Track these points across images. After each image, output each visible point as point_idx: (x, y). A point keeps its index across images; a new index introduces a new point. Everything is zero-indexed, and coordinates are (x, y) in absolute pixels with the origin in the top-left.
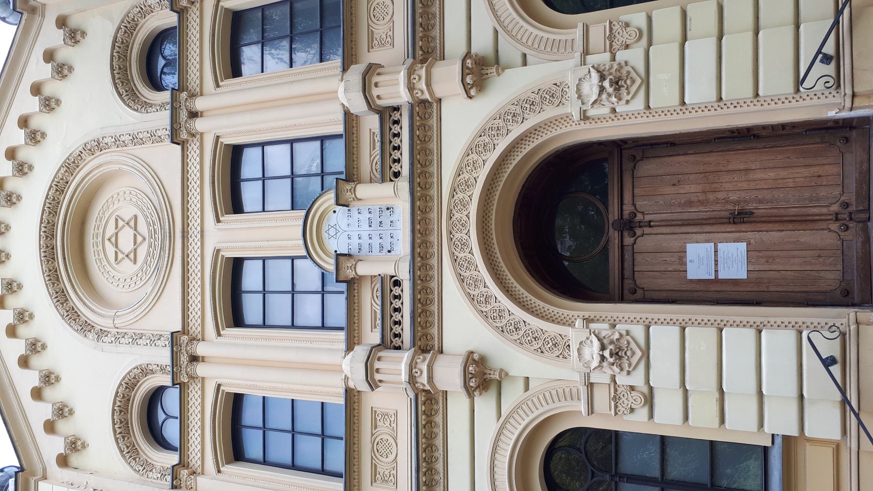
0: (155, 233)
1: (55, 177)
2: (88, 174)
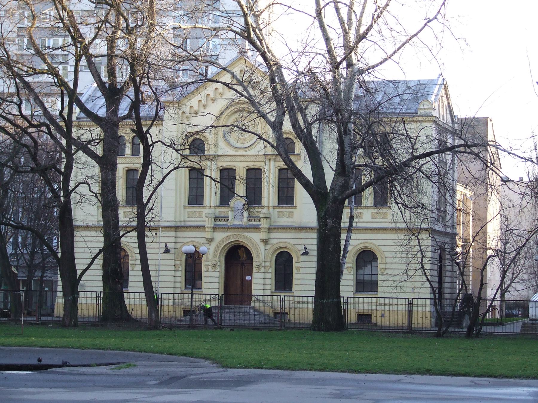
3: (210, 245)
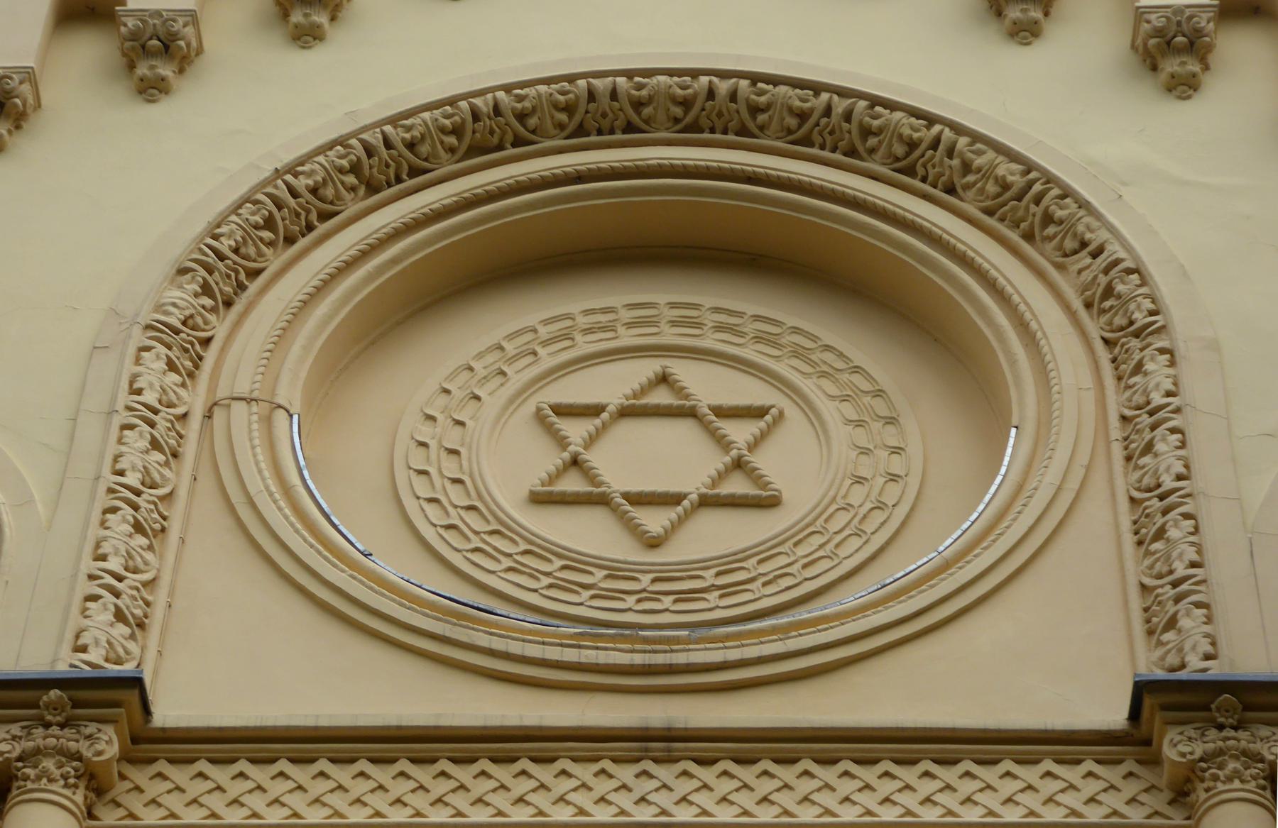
0: (682, 596)
1: (976, 137)
2: (991, 285)
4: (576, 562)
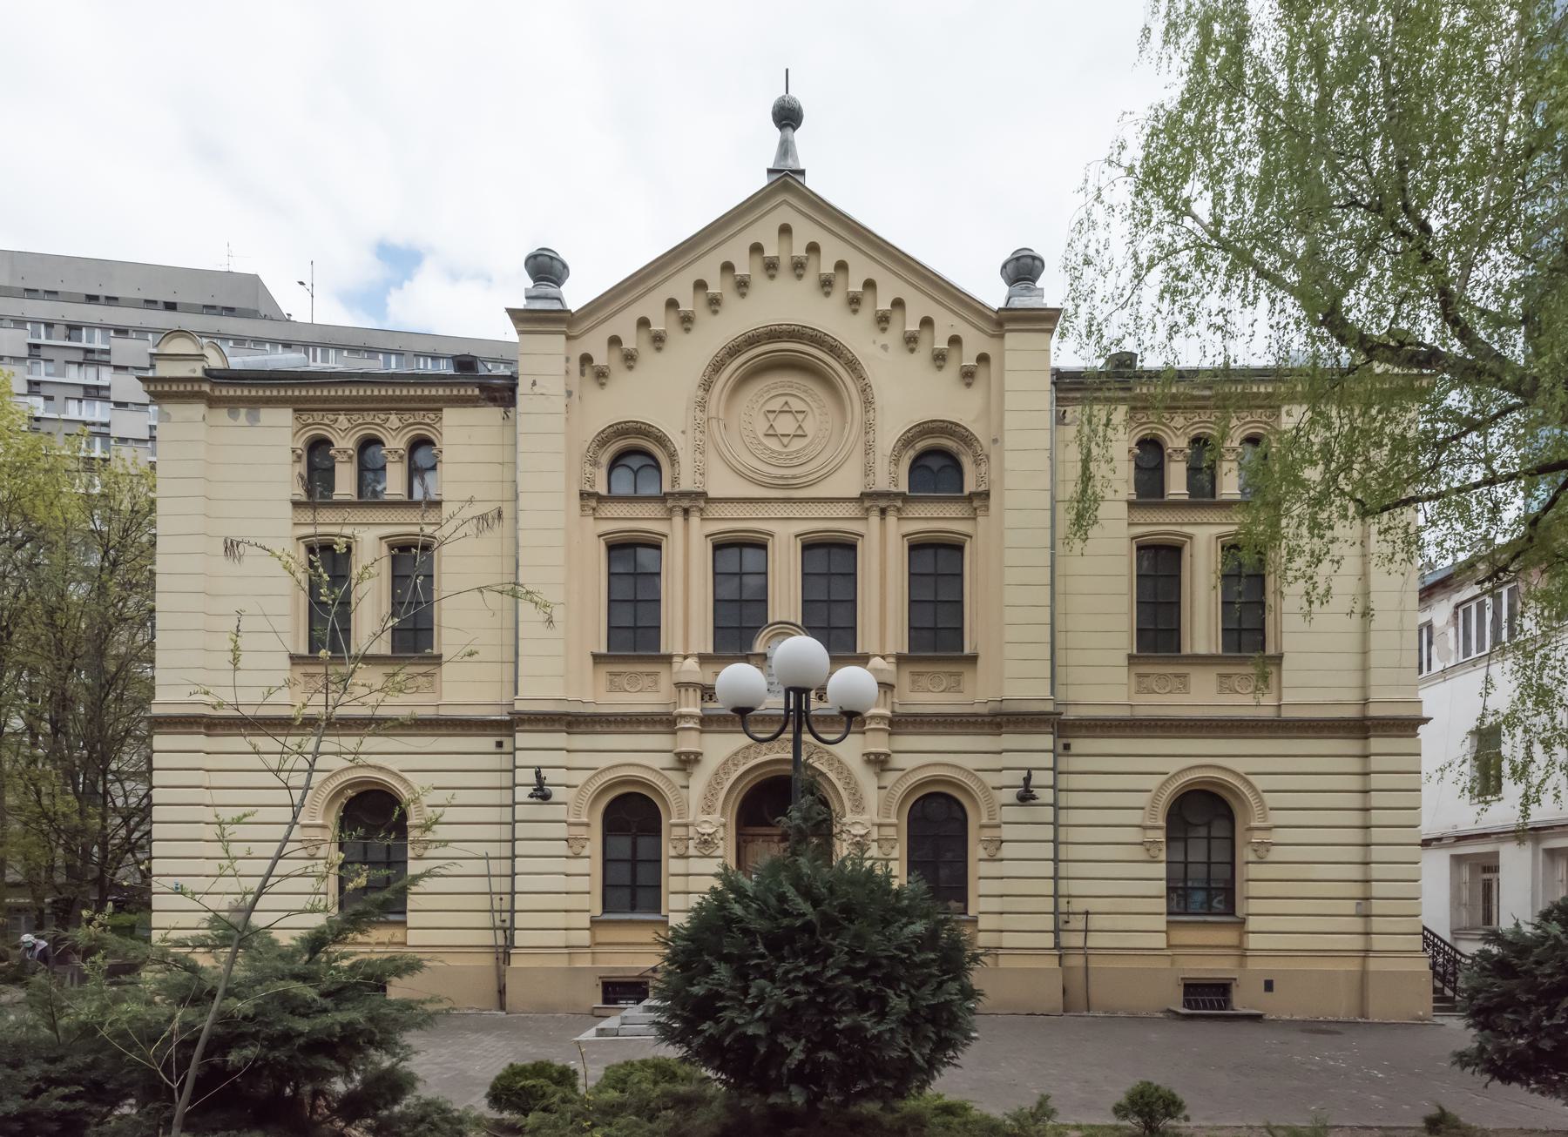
3: (689, 775)
4: (773, 451)
